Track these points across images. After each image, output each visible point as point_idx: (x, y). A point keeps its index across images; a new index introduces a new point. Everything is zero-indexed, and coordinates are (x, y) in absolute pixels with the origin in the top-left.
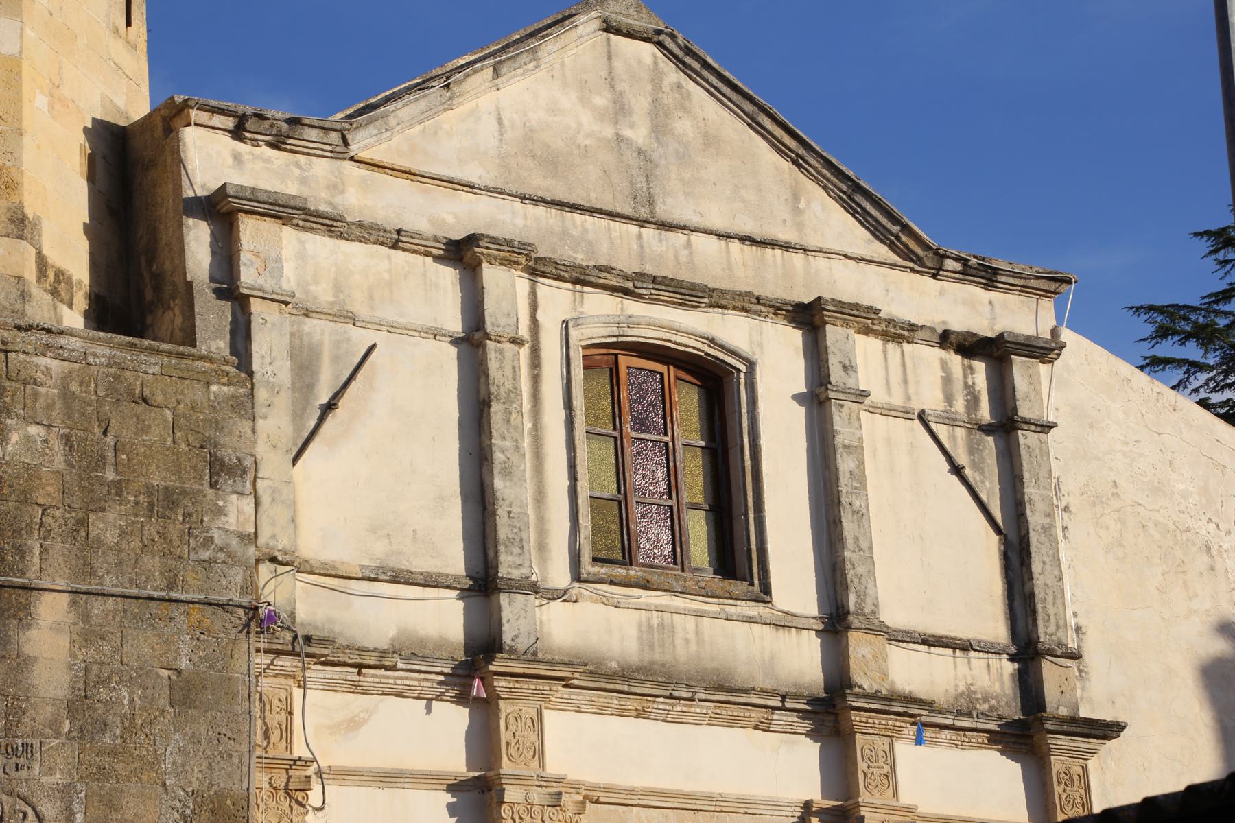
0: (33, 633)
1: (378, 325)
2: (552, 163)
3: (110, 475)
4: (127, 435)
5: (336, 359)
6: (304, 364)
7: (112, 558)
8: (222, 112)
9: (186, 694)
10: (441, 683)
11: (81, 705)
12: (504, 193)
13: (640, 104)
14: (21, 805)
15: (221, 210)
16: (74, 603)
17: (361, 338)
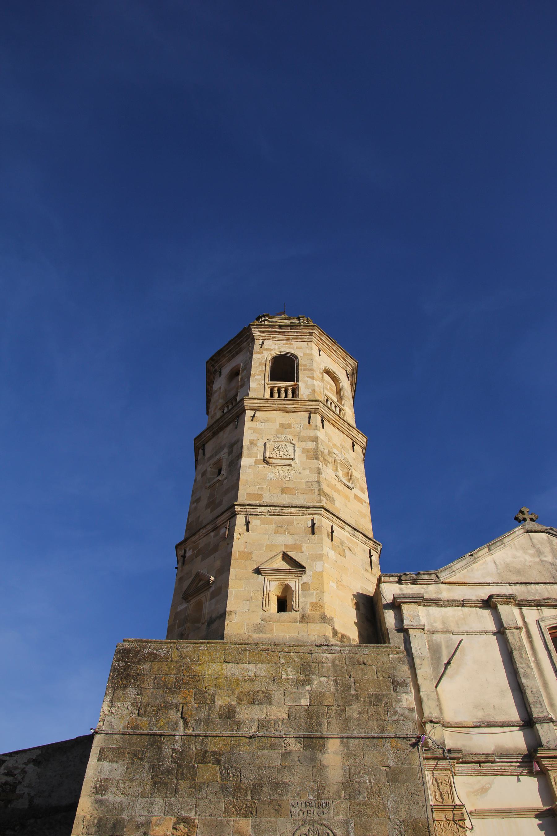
0: (326, 756)
1: (462, 633)
2: (518, 572)
3: (353, 692)
4: (358, 677)
5: (447, 647)
6: (435, 650)
7: (356, 723)
8: (392, 576)
9: (394, 777)
10: (519, 766)
11: (347, 784)
12: (501, 583)
13: (546, 550)
14: (326, 830)
15: (396, 606)
16: (342, 742)
17: (456, 638)
